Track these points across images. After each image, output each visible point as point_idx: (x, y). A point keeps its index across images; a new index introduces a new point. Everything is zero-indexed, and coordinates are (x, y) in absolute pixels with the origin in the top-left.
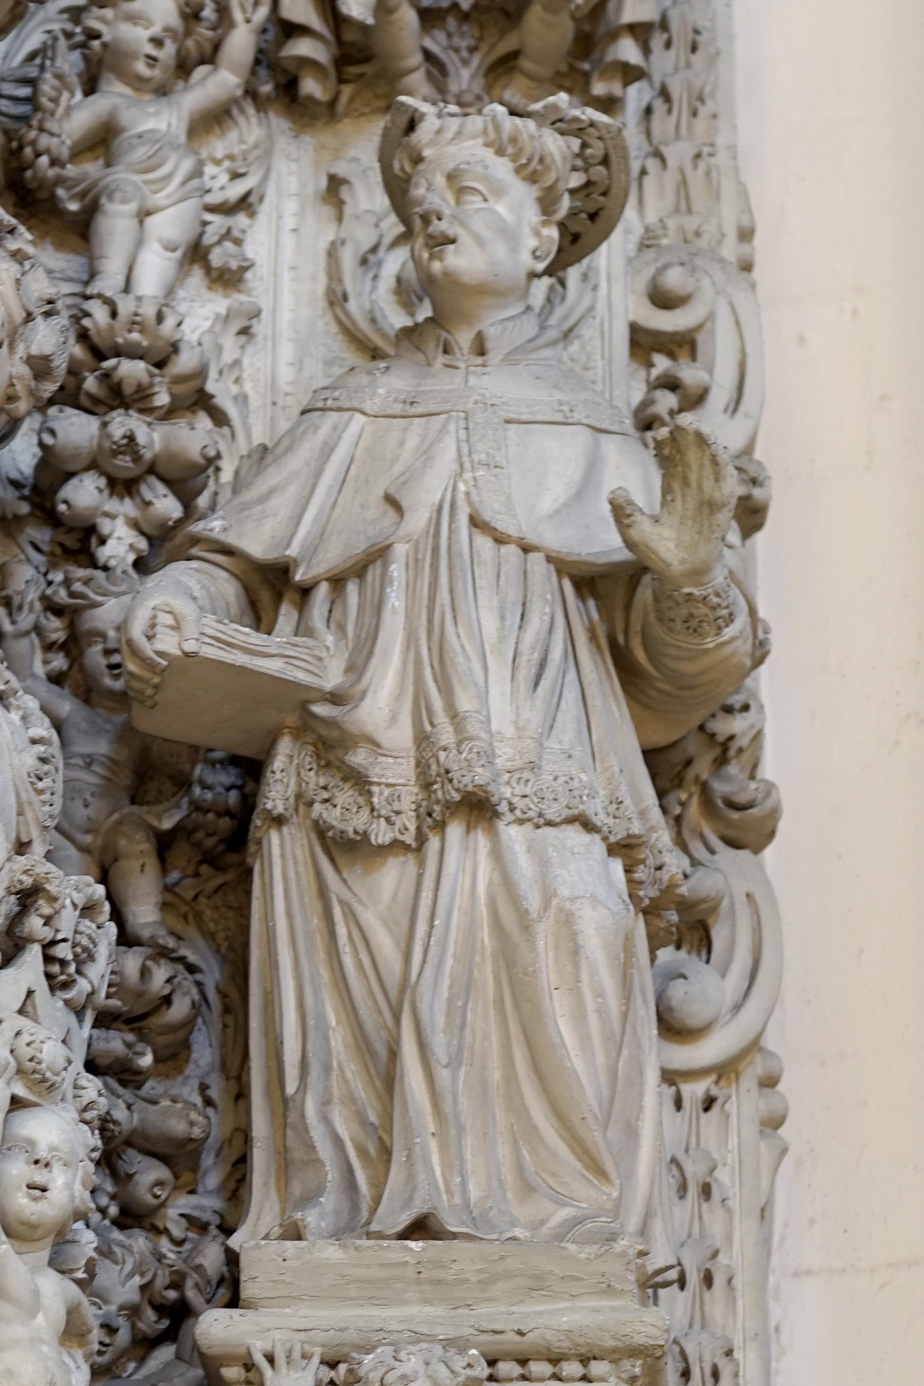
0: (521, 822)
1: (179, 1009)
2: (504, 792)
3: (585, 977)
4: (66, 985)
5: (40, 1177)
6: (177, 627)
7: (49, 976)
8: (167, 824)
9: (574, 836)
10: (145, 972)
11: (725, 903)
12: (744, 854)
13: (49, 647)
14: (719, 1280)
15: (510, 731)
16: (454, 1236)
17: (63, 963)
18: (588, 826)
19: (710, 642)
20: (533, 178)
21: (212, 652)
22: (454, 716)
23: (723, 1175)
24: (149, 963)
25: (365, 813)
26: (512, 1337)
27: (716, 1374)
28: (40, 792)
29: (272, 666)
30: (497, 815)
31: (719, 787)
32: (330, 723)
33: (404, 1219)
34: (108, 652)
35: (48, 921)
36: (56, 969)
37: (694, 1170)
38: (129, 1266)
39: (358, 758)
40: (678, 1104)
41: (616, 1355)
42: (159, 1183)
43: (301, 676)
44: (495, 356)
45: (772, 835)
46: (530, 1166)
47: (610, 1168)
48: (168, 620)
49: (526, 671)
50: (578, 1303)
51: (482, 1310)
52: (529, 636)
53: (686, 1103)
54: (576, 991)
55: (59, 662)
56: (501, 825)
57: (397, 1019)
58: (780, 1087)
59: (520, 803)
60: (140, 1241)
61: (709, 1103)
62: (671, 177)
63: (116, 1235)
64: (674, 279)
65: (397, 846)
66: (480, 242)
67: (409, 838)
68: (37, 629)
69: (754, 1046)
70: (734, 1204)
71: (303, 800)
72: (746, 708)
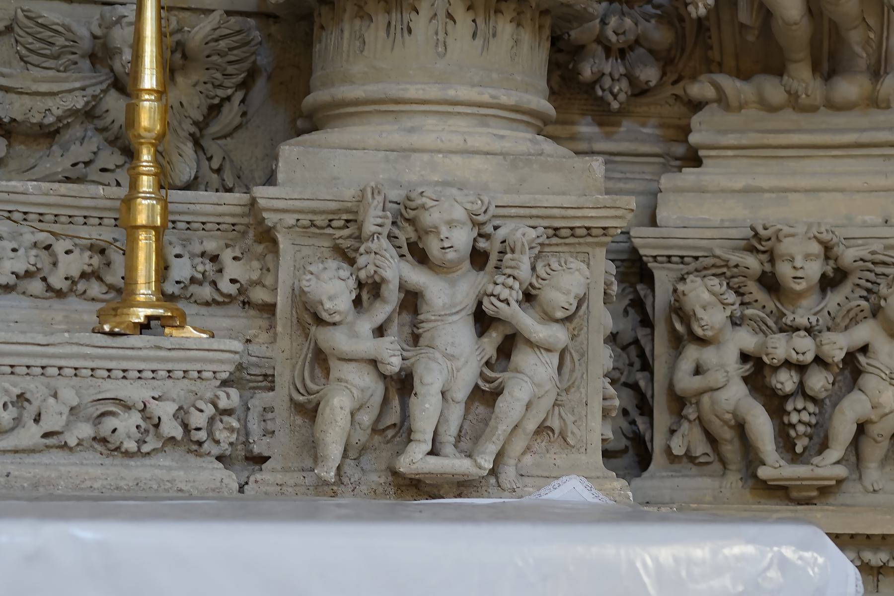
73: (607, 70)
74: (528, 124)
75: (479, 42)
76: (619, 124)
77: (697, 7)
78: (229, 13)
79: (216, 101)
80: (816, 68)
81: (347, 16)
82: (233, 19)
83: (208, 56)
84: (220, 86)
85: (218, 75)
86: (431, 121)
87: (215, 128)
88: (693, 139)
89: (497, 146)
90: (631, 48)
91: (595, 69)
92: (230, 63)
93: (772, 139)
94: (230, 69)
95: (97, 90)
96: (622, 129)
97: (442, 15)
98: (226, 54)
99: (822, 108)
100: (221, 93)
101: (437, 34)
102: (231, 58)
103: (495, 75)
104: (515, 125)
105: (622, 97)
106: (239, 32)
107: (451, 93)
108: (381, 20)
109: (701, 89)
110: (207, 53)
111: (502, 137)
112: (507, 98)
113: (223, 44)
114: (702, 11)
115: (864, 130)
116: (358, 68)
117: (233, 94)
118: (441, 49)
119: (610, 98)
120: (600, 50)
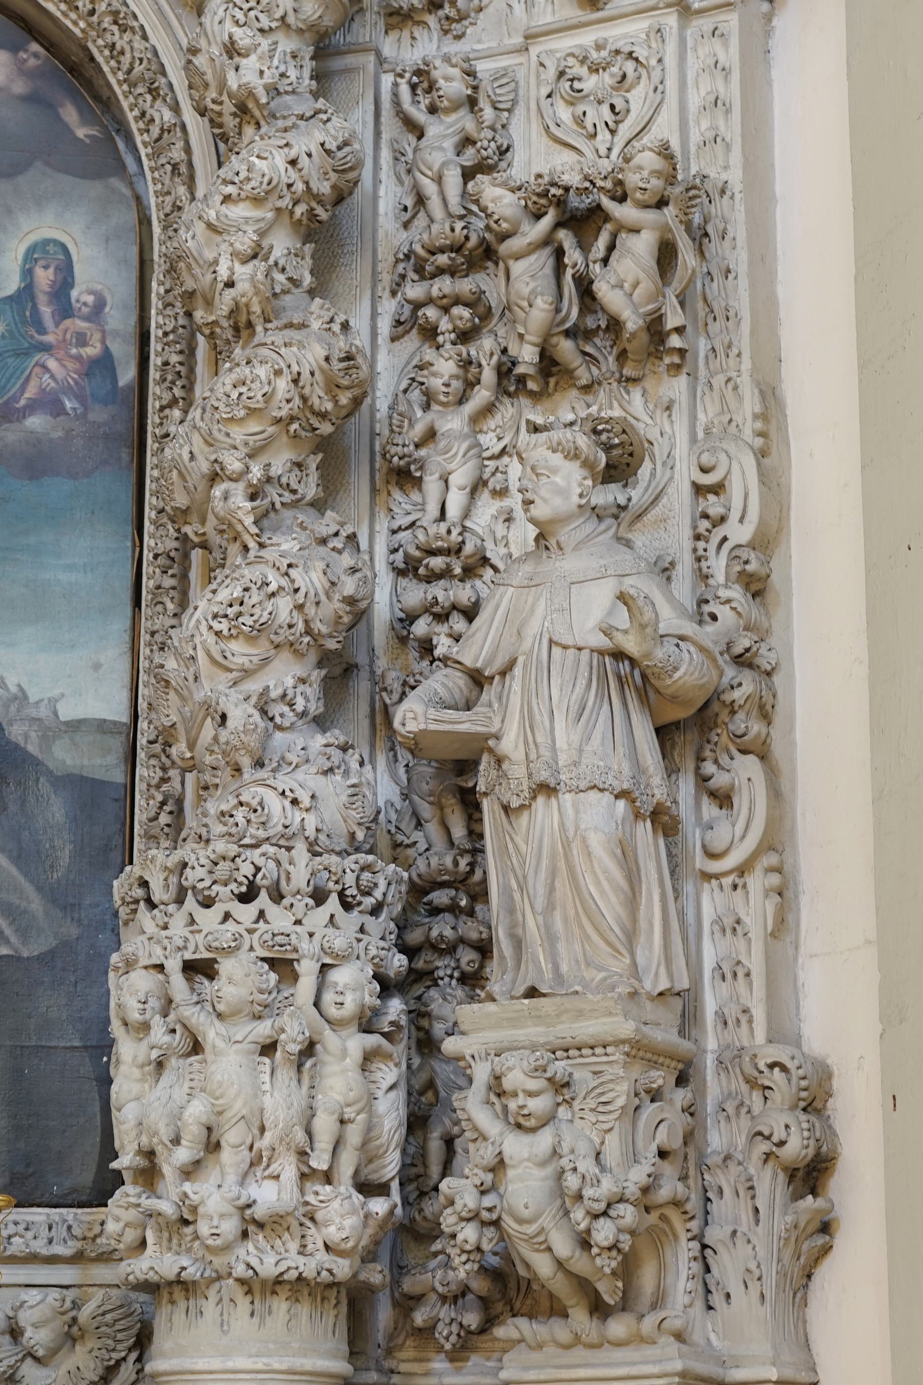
3: (596, 865)
9: (593, 795)
10: (456, 863)
15: (565, 747)
16: (544, 995)
20: (576, 457)
21: (433, 727)
24: (458, 858)
43: (480, 729)
44: (567, 550)
48: (411, 715)
50: (599, 1021)
51: (560, 1027)
53: (725, 888)
56: (560, 795)
62: (716, 394)
64: (706, 459)
65: (522, 807)
66: (545, 501)
73: (441, 1316)
75: (256, 1319)
76: (467, 1359)
79: (112, 1363)
83: (97, 1328)
84: (114, 1350)
85: (110, 1342)
92: (119, 1331)
94: (120, 1336)
95: (12, 1361)
97: (226, 1300)
100: (116, 1356)
101: (222, 1314)
102: (118, 1327)
103: (271, 1346)
107: (230, 1365)
108: (182, 1304)
110: (95, 1325)
113: (109, 1317)
115: (634, 1364)
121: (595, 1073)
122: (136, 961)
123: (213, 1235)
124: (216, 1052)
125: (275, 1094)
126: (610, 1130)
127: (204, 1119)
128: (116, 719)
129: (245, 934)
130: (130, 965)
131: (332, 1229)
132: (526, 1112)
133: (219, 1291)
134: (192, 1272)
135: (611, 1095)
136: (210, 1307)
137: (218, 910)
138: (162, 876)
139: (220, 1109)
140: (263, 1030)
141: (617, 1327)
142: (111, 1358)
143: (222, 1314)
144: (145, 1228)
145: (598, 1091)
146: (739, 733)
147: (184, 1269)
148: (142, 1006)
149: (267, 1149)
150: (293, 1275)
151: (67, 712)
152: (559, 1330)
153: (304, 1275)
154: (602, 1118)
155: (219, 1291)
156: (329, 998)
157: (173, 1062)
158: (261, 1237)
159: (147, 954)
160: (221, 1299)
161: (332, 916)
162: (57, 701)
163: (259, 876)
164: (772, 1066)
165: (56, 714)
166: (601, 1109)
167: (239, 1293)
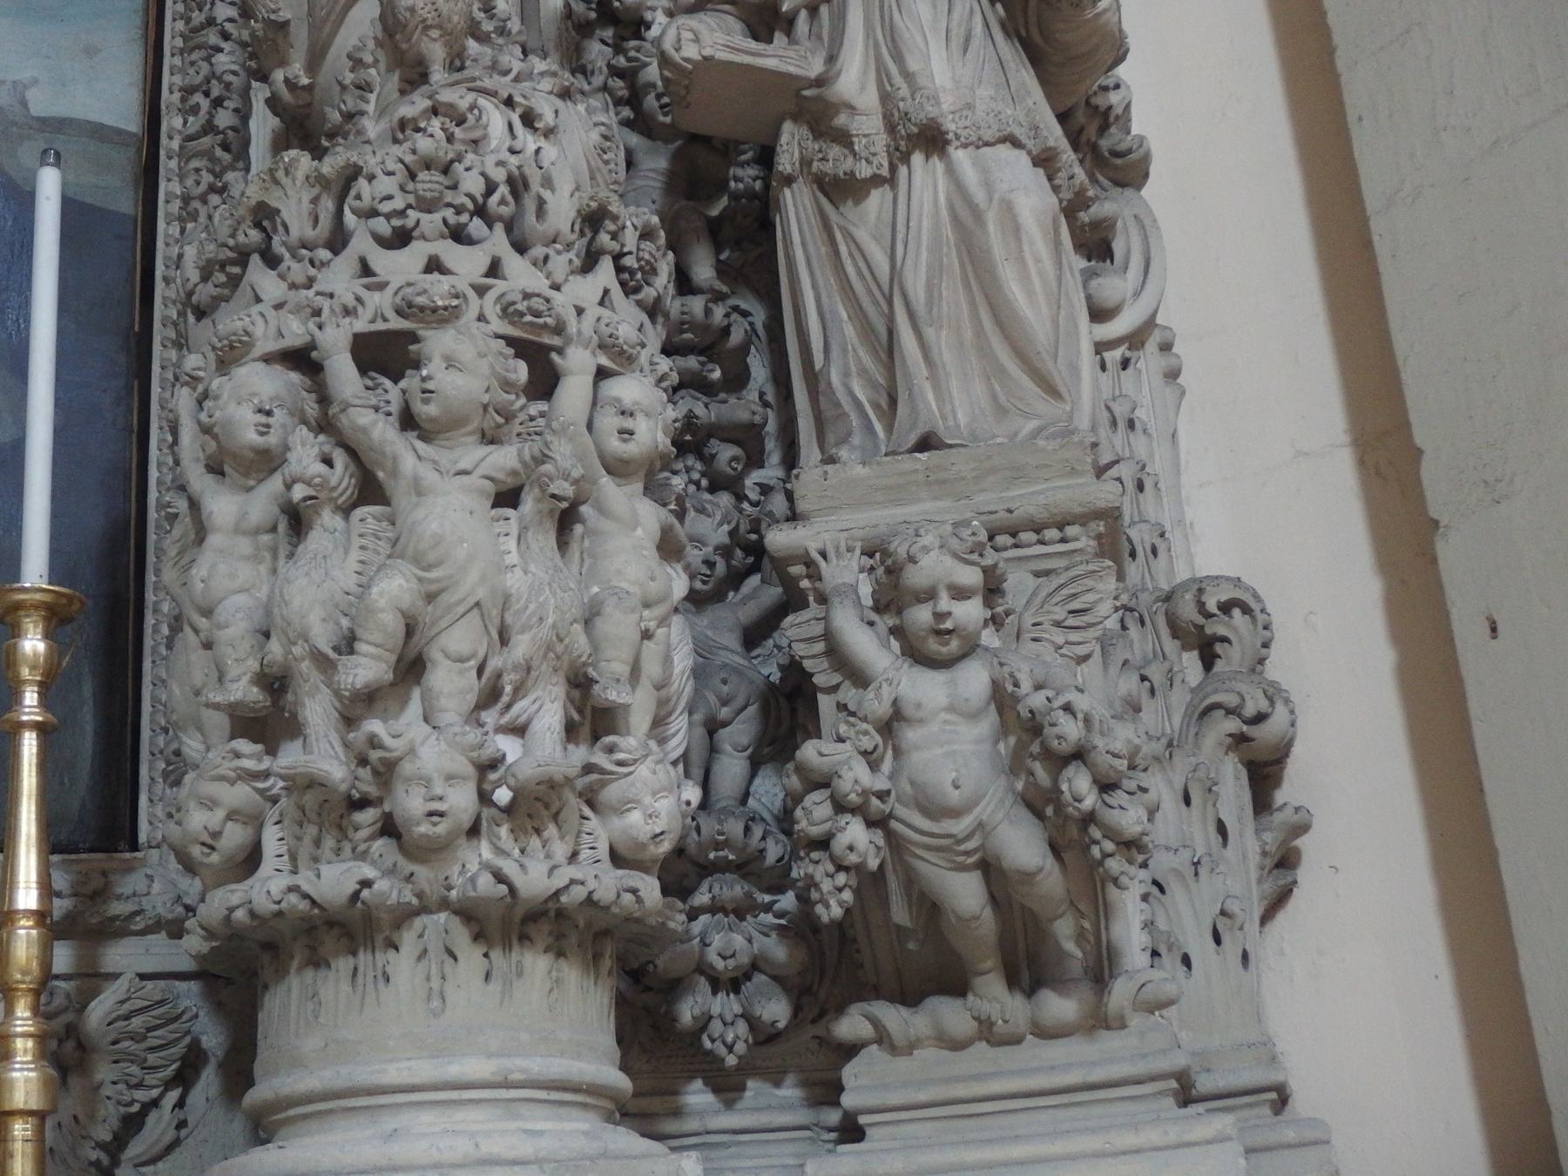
0: (965, 146)
1: (736, 337)
2: (950, 126)
3: (1026, 247)
4: (637, 290)
5: (628, 423)
6: (697, 40)
7: (623, 284)
8: (715, 212)
9: (1005, 151)
10: (708, 312)
11: (1119, 224)
12: (1129, 192)
13: (618, 102)
14: (1148, 485)
15: (949, 85)
16: (951, 446)
17: (632, 272)
18: (1016, 143)
19: (1089, 14)
22: (908, 76)
23: (1140, 414)
24: (710, 305)
25: (850, 159)
26: (1002, 514)
27: (1154, 552)
28: (607, 162)
29: (771, 63)
30: (947, 142)
31: (1105, 144)
32: (819, 99)
33: (913, 439)
34: (659, 97)
35: (614, 236)
36: (626, 276)
37: (1120, 410)
38: (718, 517)
39: (841, 120)
40: (1103, 368)
41: (1083, 519)
42: (735, 459)
43: (792, 69)
45: (1147, 175)
46: (1002, 398)
47: (1062, 389)
48: (690, 35)
49: (956, 43)
50: (1050, 485)
52: (956, 16)
53: (1109, 365)
54: (1021, 260)
55: (627, 112)
56: (951, 149)
57: (890, 302)
58: (1175, 350)
59: (963, 133)
60: (725, 499)
61: (1125, 364)
63: (707, 496)
65: (876, 181)
67: (885, 172)
68: (605, 88)
69: (1150, 324)
70: (1152, 431)
71: (806, 163)
72: (1117, 86)
73: (716, 1009)
74: (584, 1106)
75: (495, 986)
77: (827, 906)
78: (143, 977)
79: (135, 1108)
80: (1012, 981)
81: (295, 963)
82: (150, 985)
83: (114, 1043)
85: (134, 1069)
86: (426, 1118)
87: (137, 1148)
88: (848, 1100)
89: (526, 1148)
90: (747, 977)
91: (697, 1012)
92: (152, 1049)
93: (961, 1091)
94: (152, 1059)
96: (748, 1094)
98: (145, 1038)
99: (1030, 1037)
101: (428, 979)
103: (525, 1037)
104: (563, 1111)
105: (740, 1048)
106: (161, 1003)
109: (851, 1025)
110: (110, 1038)
111: (540, 1133)
112: (537, 1066)
113: (137, 1023)
114: (837, 912)
116: (311, 1044)
117: (162, 1095)
118: (436, 1003)
119: (722, 1051)
120: (703, 985)
121: (1037, 574)
122: (248, 346)
123: (431, 814)
124: (419, 489)
125: (532, 568)
126: (1086, 658)
127: (406, 601)
128: (123, 126)
129: (471, 294)
130: (229, 356)
131: (635, 817)
132: (948, 625)
133: (421, 936)
134: (388, 891)
135: (1090, 597)
136: (402, 963)
137: (417, 253)
138: (306, 198)
139: (433, 588)
140: (504, 458)
141: (1060, 1006)
142: (132, 1102)
143: (428, 979)
144: (261, 825)
145: (1065, 592)
146: (1123, 147)
147: (366, 883)
148: (263, 419)
149: (515, 668)
150: (579, 893)
151: (41, 103)
152: (951, 1014)
153: (596, 897)
154: (1074, 636)
155: (421, 936)
156: (609, 422)
157: (329, 519)
158: (504, 831)
159: (272, 330)
160: (425, 951)
161: (606, 292)
162: (25, 87)
163: (495, 198)
164: (1226, 607)
165: (24, 103)
166: (1071, 622)
167: (461, 936)
